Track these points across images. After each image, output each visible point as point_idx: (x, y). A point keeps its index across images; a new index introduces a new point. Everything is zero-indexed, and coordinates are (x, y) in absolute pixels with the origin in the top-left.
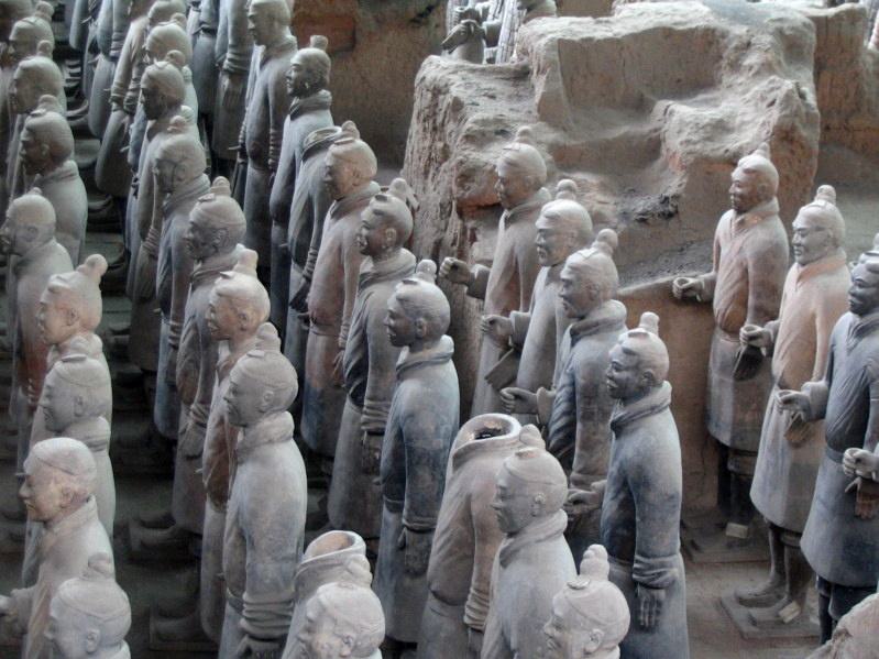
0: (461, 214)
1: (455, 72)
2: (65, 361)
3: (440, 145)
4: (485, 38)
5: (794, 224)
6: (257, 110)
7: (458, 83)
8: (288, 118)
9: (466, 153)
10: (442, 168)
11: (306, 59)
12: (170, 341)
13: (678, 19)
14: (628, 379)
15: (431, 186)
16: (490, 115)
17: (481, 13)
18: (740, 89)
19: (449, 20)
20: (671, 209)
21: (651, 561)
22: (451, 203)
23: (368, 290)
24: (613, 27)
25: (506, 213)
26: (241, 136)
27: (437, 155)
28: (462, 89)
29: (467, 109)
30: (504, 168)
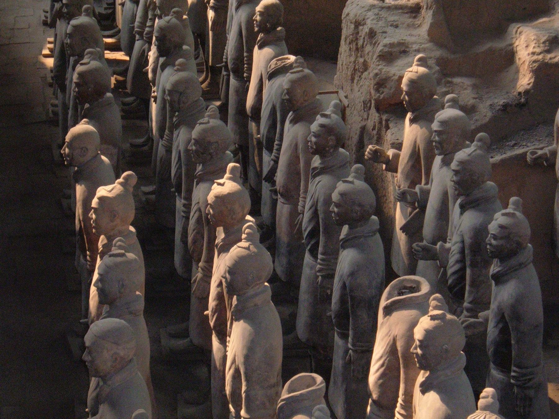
0: (378, 109)
1: (369, 10)
2: (110, 256)
3: (361, 60)
6: (234, 41)
7: (371, 18)
8: (256, 47)
9: (380, 67)
10: (363, 76)
12: (182, 214)
14: (502, 245)
15: (356, 88)
16: (395, 40)
21: (524, 371)
22: (370, 101)
23: (318, 179)
25: (409, 115)
26: (224, 57)
27: (359, 66)
28: (374, 22)
29: (379, 37)
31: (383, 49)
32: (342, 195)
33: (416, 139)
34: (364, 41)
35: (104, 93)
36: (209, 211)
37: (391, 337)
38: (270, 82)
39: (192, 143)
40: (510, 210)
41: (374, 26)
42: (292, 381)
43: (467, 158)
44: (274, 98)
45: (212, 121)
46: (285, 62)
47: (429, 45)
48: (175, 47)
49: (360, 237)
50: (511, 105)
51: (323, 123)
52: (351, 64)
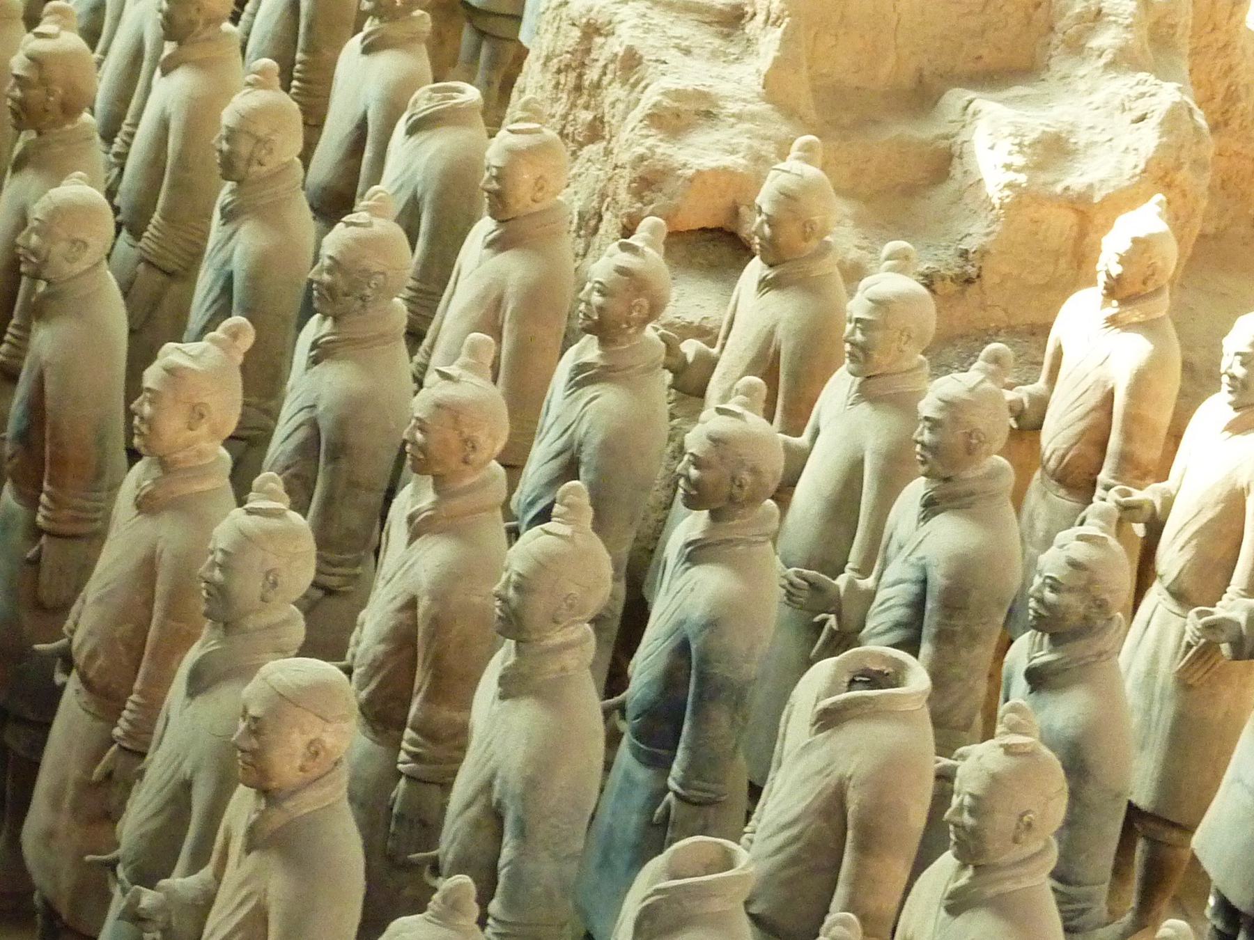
3: (587, 116)
6: (276, 17)
9: (650, 142)
14: (1068, 607)
20: (972, 271)
23: (589, 391)
25: (755, 269)
28: (638, 32)
29: (650, 70)
30: (776, 202)
31: (660, 101)
32: (717, 441)
33: (775, 326)
34: (604, 74)
35: (80, 112)
36: (412, 434)
37: (832, 780)
38: (412, 139)
39: (322, 266)
40: (1091, 528)
41: (635, 43)
42: (676, 851)
43: (966, 396)
44: (419, 178)
45: (376, 221)
47: (762, 107)
48: (208, 22)
50: (943, 279)
52: (554, 120)
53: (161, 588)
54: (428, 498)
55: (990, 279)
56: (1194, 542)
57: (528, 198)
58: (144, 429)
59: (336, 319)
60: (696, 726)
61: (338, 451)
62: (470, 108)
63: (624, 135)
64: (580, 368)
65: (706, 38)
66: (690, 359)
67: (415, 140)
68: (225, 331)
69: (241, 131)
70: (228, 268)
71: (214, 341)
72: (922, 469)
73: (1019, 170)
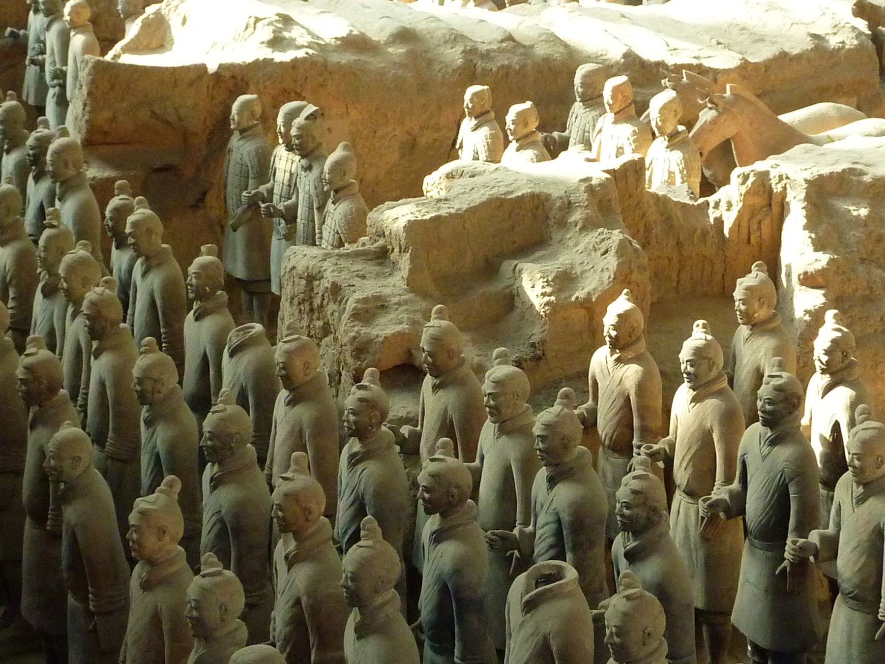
3: (319, 323)
4: (283, 217)
5: (681, 356)
7: (331, 269)
9: (356, 328)
11: (204, 267)
13: (503, 190)
17: (265, 195)
18: (571, 244)
19: (231, 202)
20: (539, 352)
23: (360, 467)
24: (452, 204)
25: (428, 381)
32: (434, 476)
35: (58, 389)
36: (276, 513)
41: (336, 279)
43: (556, 419)
45: (228, 407)
46: (249, 332)
49: (459, 525)
50: (526, 361)
51: (363, 397)
53: (165, 627)
54: (292, 545)
55: (550, 354)
56: (691, 463)
57: (302, 375)
58: (136, 547)
59: (220, 464)
60: (460, 628)
61: (238, 531)
62: (259, 335)
63: (342, 328)
64: (352, 456)
65: (370, 268)
66: (407, 436)
67: (235, 359)
68: (165, 485)
69: (145, 378)
70: (156, 450)
71: (161, 492)
72: (543, 463)
73: (549, 295)
